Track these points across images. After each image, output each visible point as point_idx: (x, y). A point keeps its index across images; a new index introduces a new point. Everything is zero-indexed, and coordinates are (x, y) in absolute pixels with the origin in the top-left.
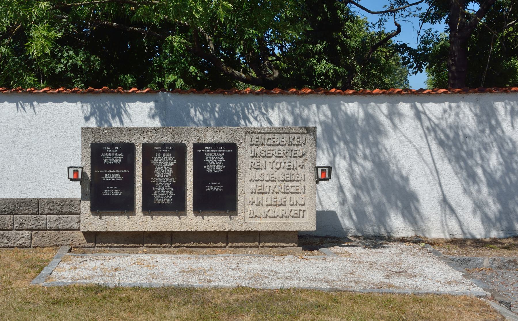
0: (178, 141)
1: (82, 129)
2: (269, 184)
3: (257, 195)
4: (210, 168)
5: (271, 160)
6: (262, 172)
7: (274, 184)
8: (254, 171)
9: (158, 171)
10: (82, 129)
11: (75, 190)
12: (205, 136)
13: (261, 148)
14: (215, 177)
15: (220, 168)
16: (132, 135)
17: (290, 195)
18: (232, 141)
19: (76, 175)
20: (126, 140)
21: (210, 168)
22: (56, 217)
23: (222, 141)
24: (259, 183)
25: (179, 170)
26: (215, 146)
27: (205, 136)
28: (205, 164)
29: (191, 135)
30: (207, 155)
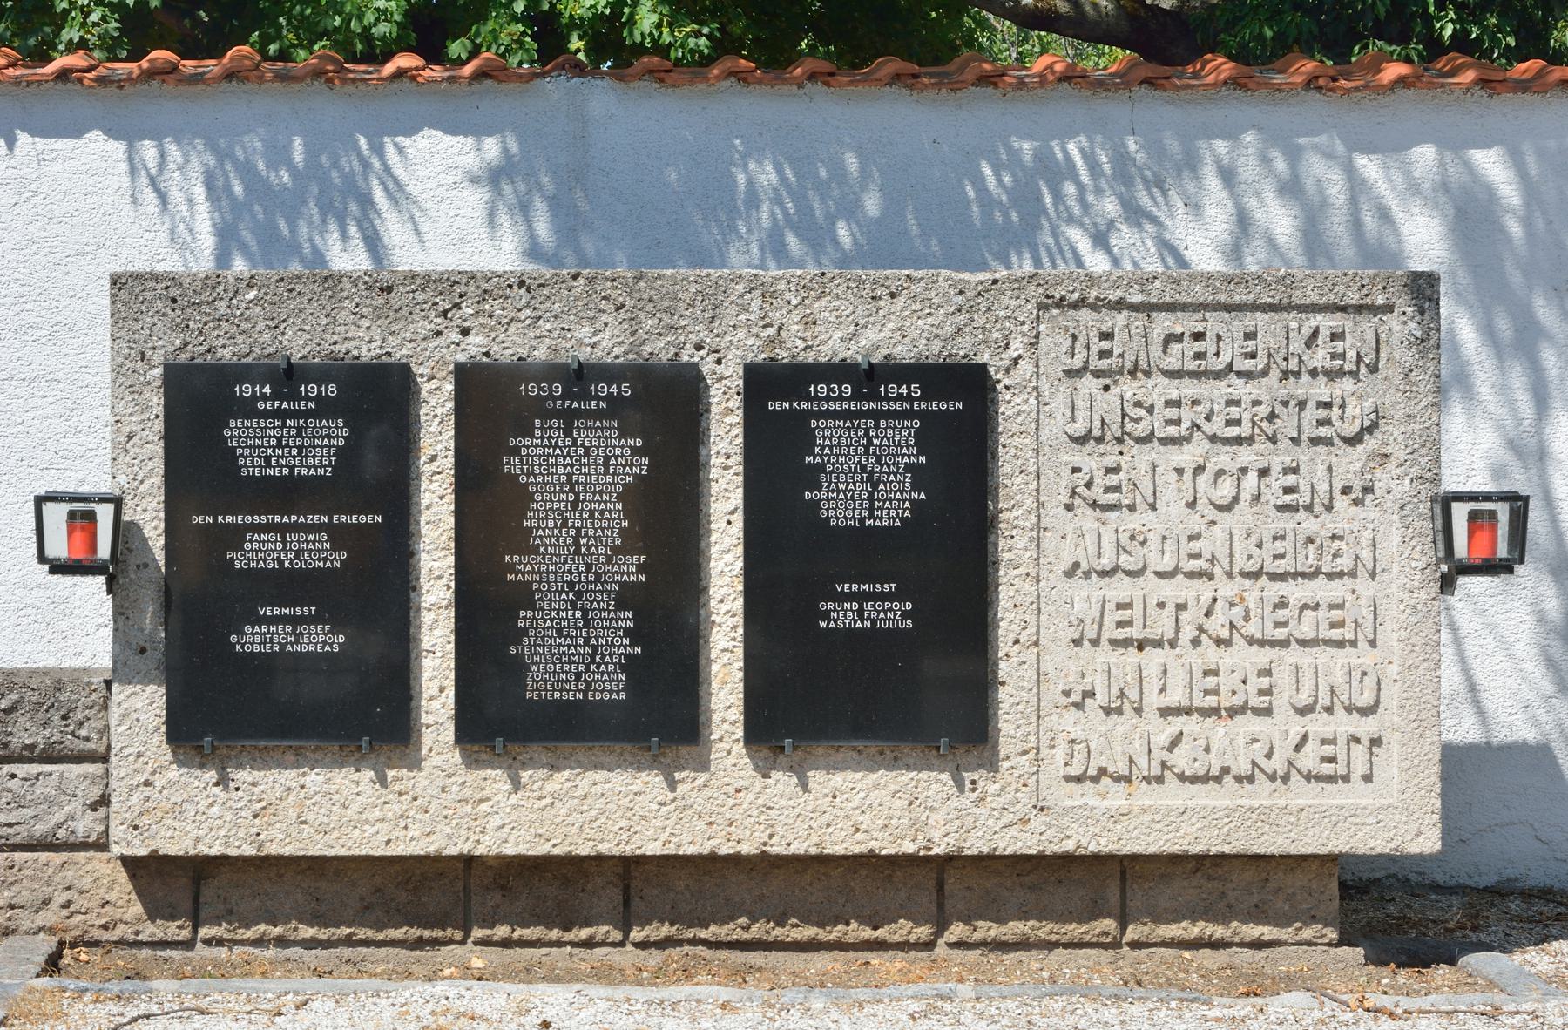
0: (659, 349)
1: (116, 281)
4: (840, 503)
5: (1186, 456)
6: (1133, 522)
7: (1204, 590)
8: (1087, 519)
9: (544, 519)
10: (116, 281)
12: (809, 322)
13: (1129, 388)
14: (865, 551)
15: (896, 503)
18: (962, 348)
20: (364, 341)
21: (840, 503)
23: (904, 353)
24: (1121, 588)
26: (868, 378)
27: (809, 322)
28: (812, 476)
29: (729, 315)
30: (824, 430)
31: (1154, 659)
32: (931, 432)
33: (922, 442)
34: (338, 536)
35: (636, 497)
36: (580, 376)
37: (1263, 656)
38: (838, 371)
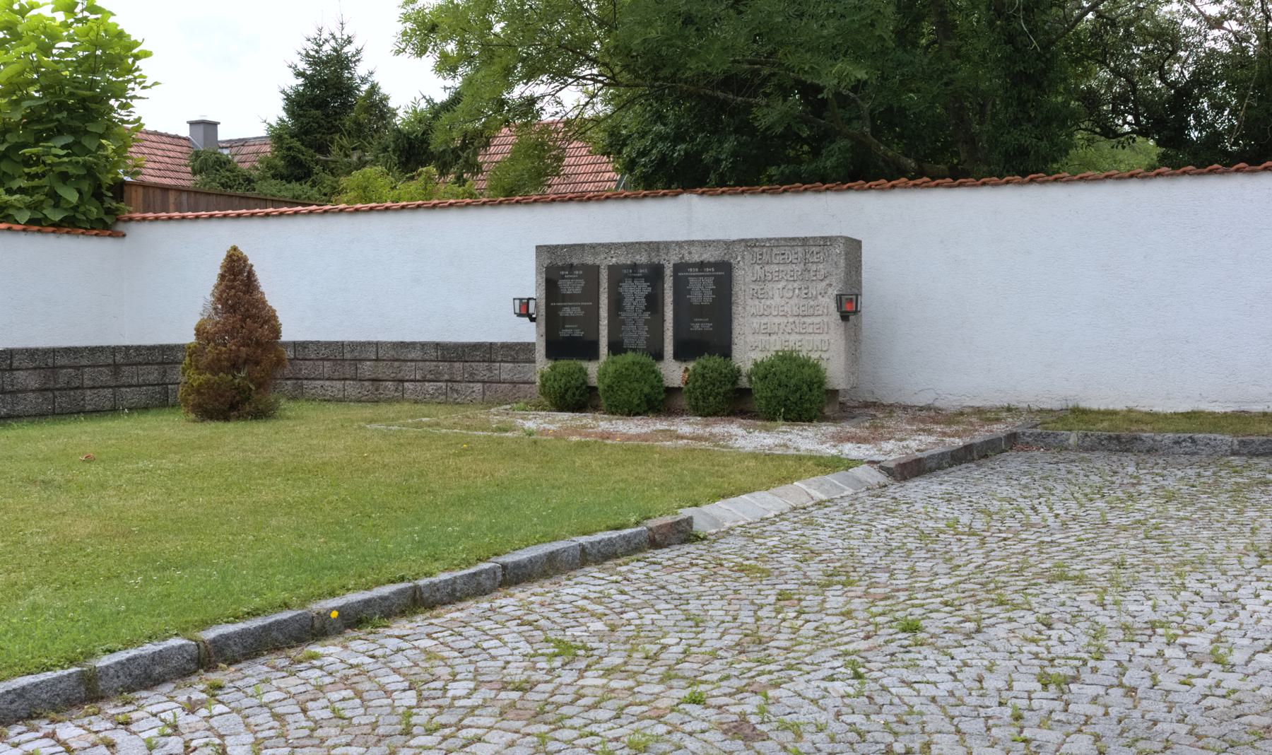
0: (655, 260)
1: (538, 247)
2: (776, 320)
3: (761, 337)
4: (695, 298)
5: (781, 285)
6: (768, 303)
7: (785, 320)
8: (757, 302)
9: (627, 303)
10: (538, 247)
11: (529, 333)
12: (690, 253)
13: (767, 268)
14: (701, 311)
15: (708, 298)
16: (596, 254)
17: (808, 337)
18: (726, 258)
19: (524, 310)
20: (589, 260)
21: (695, 298)
22: (511, 365)
23: (712, 260)
24: (765, 320)
25: (654, 303)
26: (702, 265)
27: (690, 253)
28: (689, 291)
29: (672, 252)
30: (691, 280)
31: (774, 337)
32: (717, 281)
33: (715, 283)
34: (583, 308)
35: (648, 297)
36: (635, 267)
37: (799, 337)
38: (694, 265)
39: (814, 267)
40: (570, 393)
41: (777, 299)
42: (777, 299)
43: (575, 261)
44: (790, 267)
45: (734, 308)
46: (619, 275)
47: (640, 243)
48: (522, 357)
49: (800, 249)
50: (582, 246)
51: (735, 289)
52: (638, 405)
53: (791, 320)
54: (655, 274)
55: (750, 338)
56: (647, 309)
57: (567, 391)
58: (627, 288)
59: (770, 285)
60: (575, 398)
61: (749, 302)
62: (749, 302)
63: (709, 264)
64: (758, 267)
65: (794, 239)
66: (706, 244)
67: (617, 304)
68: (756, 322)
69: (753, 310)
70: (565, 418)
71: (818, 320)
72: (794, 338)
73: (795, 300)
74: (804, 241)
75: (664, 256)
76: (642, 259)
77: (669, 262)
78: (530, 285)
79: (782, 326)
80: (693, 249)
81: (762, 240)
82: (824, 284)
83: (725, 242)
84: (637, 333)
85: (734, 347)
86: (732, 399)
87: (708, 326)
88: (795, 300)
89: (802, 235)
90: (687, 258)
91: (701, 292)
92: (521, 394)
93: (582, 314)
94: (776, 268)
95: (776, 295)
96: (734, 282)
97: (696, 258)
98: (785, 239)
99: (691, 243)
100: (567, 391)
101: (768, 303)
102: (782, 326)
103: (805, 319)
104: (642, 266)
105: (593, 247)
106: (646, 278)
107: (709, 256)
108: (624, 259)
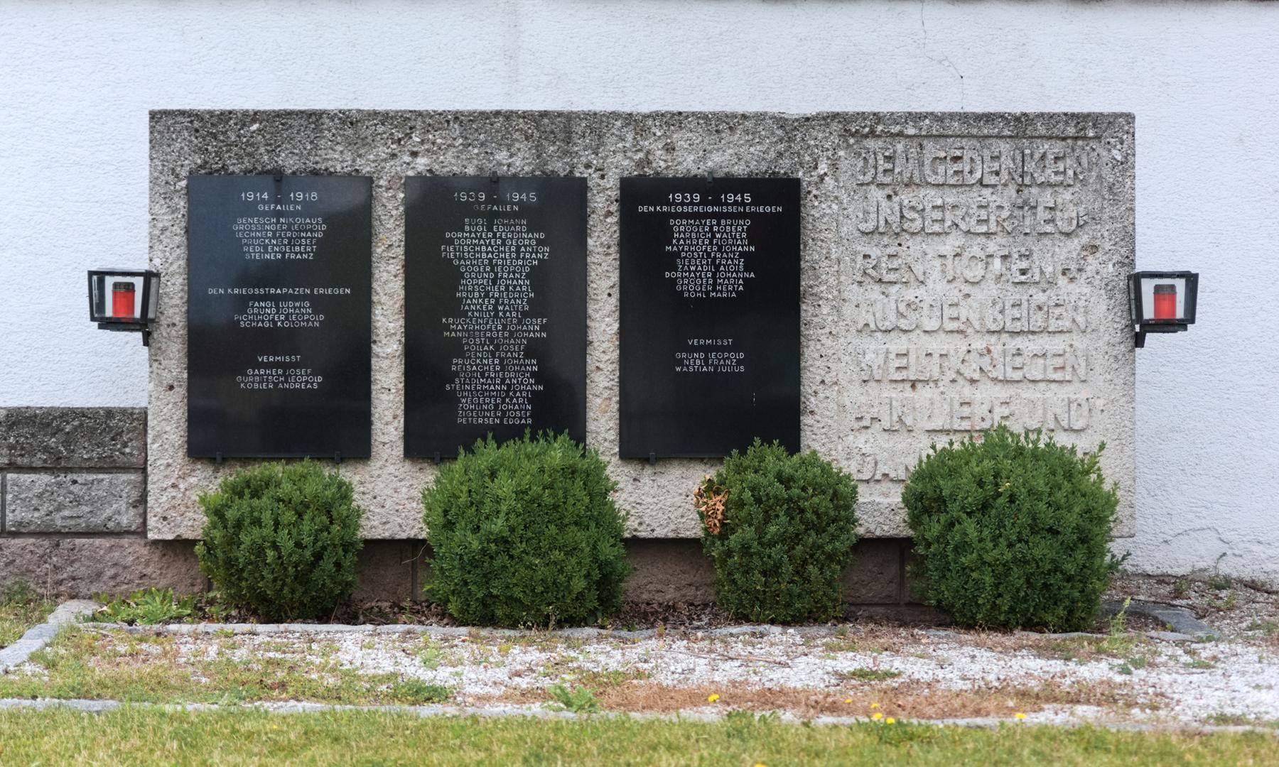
0: (558, 167)
1: (154, 116)
2: (936, 344)
3: (888, 392)
4: (691, 279)
5: (949, 245)
6: (910, 294)
7: (960, 344)
8: (875, 292)
9: (472, 292)
10: (154, 116)
11: (128, 376)
12: (670, 149)
13: (906, 197)
14: (709, 314)
15: (733, 280)
16: (359, 144)
17: (1027, 392)
18: (783, 167)
19: (118, 304)
20: (338, 159)
21: (691, 279)
22: (45, 479)
23: (739, 170)
24: (899, 344)
25: (559, 291)
26: (713, 188)
27: (670, 149)
28: (671, 261)
29: (611, 143)
30: (680, 228)
31: (925, 393)
32: (760, 230)
33: (752, 237)
34: (318, 304)
35: (538, 276)
37: (1002, 392)
38: (689, 184)
39: (1047, 198)
40: (328, 564)
41: (937, 286)
42: (937, 286)
43: (289, 162)
44: (973, 197)
45: (806, 309)
46: (435, 207)
47: (509, 116)
48: (84, 453)
49: (1004, 147)
50: (314, 118)
51: (811, 255)
52: (580, 597)
53: (979, 344)
54: (561, 202)
55: (855, 396)
56: (536, 308)
57: (318, 556)
58: (470, 247)
59: (914, 246)
60: (306, 578)
61: (853, 292)
62: (853, 292)
63: (731, 183)
64: (877, 194)
65: (989, 118)
66: (719, 124)
67: (431, 288)
68: (873, 349)
69: (864, 317)
70: (259, 642)
71: (1058, 344)
72: (987, 394)
73: (990, 290)
74: (1021, 126)
75: (587, 156)
76: (516, 160)
77: (393, 172)
78: (131, 226)
79: (954, 362)
80: (680, 139)
81: (893, 118)
82: (1075, 244)
83: (780, 121)
84: (490, 380)
85: (806, 420)
86: (799, 563)
87: (731, 362)
88: (990, 290)
89: (1017, 109)
90: (661, 163)
91: (710, 260)
92: (81, 570)
93: (316, 321)
94: (932, 197)
95: (935, 275)
96: (807, 235)
97: (688, 163)
98: (964, 117)
99: (675, 120)
100: (318, 556)
101: (910, 294)
102: (954, 362)
103: (1020, 342)
104: (518, 182)
105: (349, 120)
106: (533, 217)
107: (730, 158)
108: (454, 161)
